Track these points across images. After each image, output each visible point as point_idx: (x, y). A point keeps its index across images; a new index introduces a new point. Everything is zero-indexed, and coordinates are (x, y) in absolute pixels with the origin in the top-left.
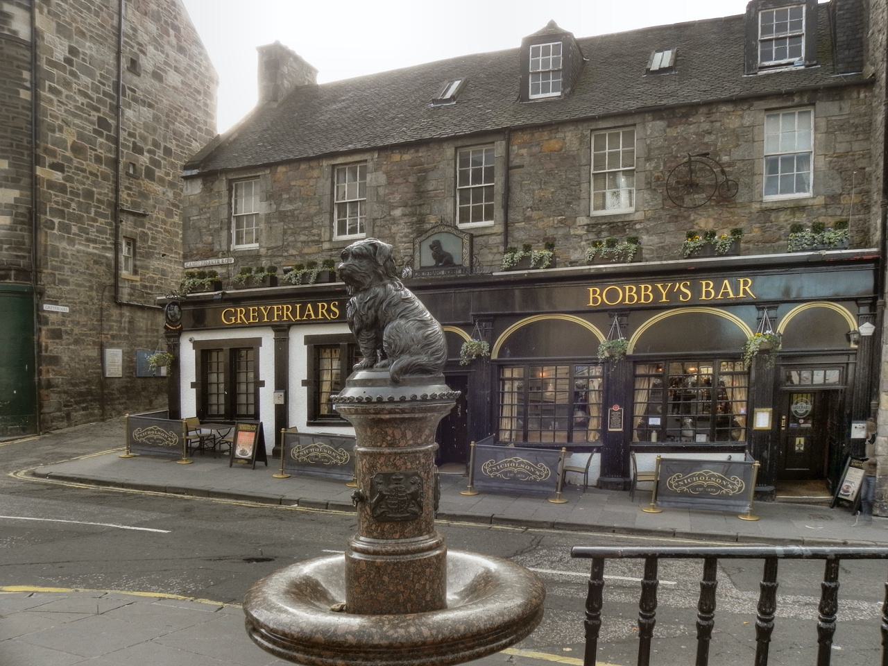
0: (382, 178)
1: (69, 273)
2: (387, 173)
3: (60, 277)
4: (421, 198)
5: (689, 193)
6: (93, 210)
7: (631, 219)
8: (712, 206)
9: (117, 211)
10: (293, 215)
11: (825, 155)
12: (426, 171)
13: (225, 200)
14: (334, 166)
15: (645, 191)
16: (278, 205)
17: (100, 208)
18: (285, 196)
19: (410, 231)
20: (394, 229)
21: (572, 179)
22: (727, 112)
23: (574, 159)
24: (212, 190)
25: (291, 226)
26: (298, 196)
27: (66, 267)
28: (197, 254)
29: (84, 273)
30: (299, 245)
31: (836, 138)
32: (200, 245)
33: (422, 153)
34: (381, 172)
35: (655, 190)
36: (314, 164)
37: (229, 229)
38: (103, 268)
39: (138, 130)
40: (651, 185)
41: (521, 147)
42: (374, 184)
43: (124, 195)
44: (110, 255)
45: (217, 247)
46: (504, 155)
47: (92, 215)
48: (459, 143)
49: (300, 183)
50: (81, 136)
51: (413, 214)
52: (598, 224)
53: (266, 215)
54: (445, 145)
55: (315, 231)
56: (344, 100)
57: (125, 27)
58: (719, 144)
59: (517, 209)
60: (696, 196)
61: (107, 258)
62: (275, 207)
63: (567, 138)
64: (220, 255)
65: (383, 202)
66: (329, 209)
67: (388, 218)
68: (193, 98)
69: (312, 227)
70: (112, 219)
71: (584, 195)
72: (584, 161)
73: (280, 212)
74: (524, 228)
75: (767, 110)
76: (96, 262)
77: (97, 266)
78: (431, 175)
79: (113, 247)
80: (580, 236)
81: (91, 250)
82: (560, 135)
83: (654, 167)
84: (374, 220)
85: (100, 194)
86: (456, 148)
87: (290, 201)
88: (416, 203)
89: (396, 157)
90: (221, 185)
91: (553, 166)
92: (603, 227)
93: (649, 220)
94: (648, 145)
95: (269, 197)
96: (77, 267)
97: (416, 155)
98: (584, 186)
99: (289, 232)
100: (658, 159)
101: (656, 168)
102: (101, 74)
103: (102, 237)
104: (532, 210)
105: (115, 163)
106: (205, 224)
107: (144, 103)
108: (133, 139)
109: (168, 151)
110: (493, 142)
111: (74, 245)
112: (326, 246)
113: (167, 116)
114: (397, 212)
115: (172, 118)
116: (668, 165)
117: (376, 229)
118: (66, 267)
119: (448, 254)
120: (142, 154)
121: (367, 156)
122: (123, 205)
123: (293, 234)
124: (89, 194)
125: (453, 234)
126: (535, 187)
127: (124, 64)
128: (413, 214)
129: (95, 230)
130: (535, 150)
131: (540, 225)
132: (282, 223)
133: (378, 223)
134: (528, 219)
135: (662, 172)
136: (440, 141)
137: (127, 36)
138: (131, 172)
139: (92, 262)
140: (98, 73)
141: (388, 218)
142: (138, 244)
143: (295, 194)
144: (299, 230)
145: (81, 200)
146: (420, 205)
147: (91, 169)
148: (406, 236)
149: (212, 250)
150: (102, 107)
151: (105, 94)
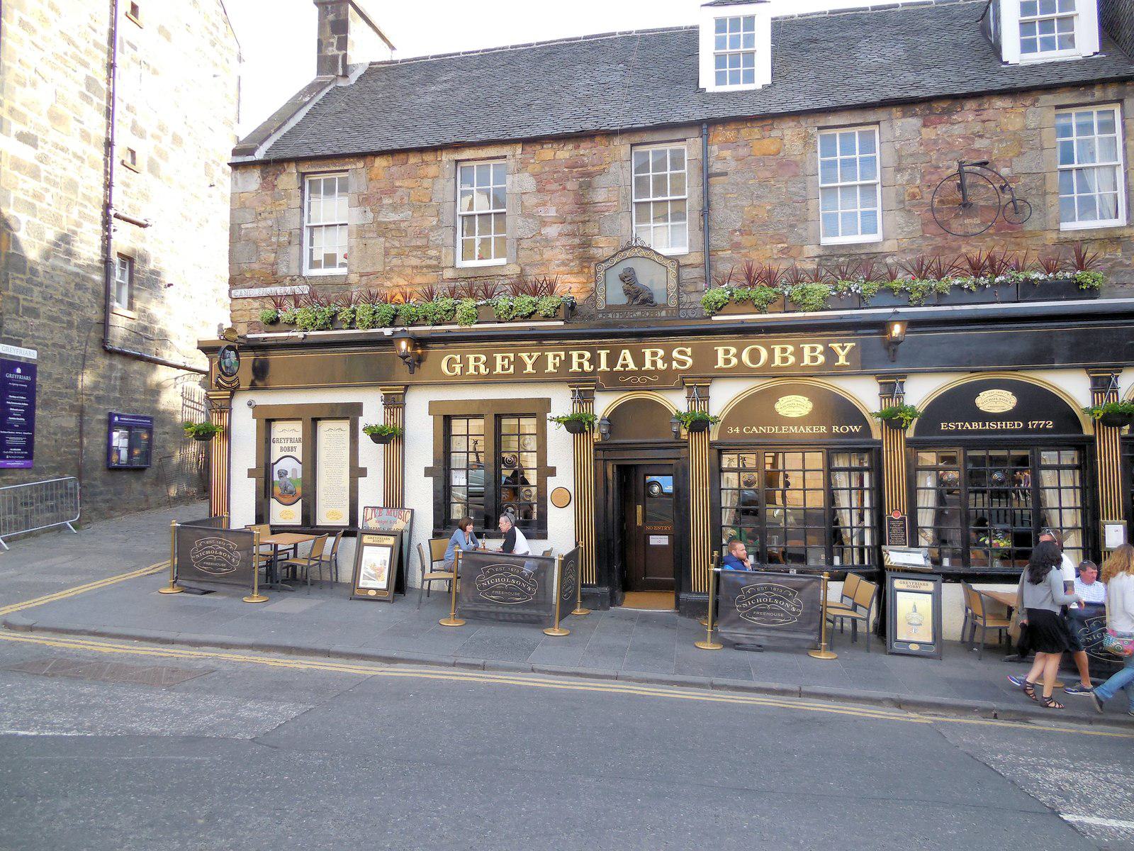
0: (529, 183)
1: (40, 299)
3: (25, 303)
4: (584, 212)
5: (957, 216)
7: (879, 250)
12: (590, 175)
13: (298, 202)
14: (457, 161)
16: (376, 212)
17: (86, 206)
19: (570, 257)
20: (548, 254)
21: (795, 194)
24: (275, 186)
25: (397, 244)
26: (406, 200)
27: (36, 290)
28: (252, 278)
29: (62, 301)
30: (409, 271)
32: (256, 266)
33: (586, 151)
34: (527, 174)
35: (909, 211)
36: (429, 157)
37: (301, 244)
38: (89, 296)
40: (907, 203)
42: (517, 190)
45: (282, 270)
46: (700, 157)
48: (636, 139)
49: (407, 183)
51: (572, 235)
52: (833, 256)
53: (358, 226)
54: (617, 141)
55: (432, 253)
56: (445, 81)
58: (995, 151)
59: (721, 232)
60: (967, 221)
61: (93, 281)
62: (371, 215)
64: (287, 281)
65: (531, 216)
66: (451, 220)
67: (538, 238)
69: (427, 247)
71: (811, 216)
72: (810, 170)
73: (380, 223)
74: (731, 258)
75: (1057, 107)
76: (79, 286)
77: (80, 293)
78: (599, 181)
79: (103, 266)
87: (394, 208)
88: (578, 219)
89: (547, 152)
91: (768, 174)
92: (842, 259)
94: (897, 151)
95: (364, 201)
96: (51, 291)
97: (576, 152)
99: (393, 252)
100: (912, 169)
101: (910, 182)
104: (742, 234)
106: (264, 235)
109: (177, 140)
112: (449, 274)
114: (552, 231)
116: (927, 178)
117: (522, 253)
118: (36, 290)
119: (646, 289)
121: (506, 150)
123: (399, 255)
126: (744, 203)
128: (573, 235)
130: (743, 152)
133: (525, 244)
134: (736, 246)
136: (610, 134)
139: (73, 285)
141: (538, 238)
142: (136, 266)
146: (584, 222)
148: (564, 264)
149: (274, 274)
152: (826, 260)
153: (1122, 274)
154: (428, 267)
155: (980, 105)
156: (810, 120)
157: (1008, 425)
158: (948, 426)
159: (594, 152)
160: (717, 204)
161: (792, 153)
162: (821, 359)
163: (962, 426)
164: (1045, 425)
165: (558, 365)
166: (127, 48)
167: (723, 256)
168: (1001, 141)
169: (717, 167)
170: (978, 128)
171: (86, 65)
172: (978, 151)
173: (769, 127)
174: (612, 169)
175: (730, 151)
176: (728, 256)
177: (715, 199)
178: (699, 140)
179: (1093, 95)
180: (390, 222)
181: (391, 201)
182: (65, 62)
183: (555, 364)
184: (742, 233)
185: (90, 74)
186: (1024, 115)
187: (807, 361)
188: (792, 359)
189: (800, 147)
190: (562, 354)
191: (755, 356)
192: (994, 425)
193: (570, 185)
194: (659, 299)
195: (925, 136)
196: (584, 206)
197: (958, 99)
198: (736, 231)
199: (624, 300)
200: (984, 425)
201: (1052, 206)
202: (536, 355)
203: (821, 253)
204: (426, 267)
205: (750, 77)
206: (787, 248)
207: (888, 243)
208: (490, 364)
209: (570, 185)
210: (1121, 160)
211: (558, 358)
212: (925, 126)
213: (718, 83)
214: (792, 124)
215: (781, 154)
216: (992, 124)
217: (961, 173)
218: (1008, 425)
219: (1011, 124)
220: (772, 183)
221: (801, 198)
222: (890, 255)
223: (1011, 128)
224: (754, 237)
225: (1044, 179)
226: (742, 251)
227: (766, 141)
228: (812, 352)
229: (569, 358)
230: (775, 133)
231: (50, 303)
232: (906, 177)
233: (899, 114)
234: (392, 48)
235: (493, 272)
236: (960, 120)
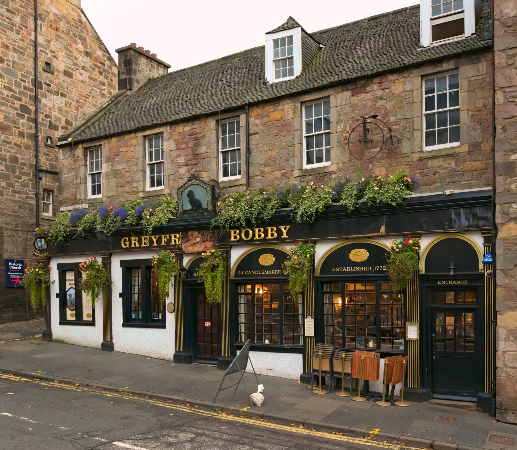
2: (175, 141)
5: (367, 148)
6: (17, 170)
8: (384, 158)
9: (38, 171)
10: (121, 173)
11: (468, 110)
13: (83, 163)
16: (113, 165)
18: (117, 159)
21: (289, 142)
22: (394, 80)
23: (290, 126)
25: (121, 181)
30: (125, 195)
31: (476, 95)
33: (197, 126)
35: (343, 147)
37: (85, 183)
39: (54, 113)
42: (168, 149)
43: (43, 159)
44: (33, 202)
45: (78, 197)
47: (17, 174)
50: (6, 118)
55: (135, 185)
57: (41, 40)
59: (255, 166)
60: (373, 150)
63: (285, 110)
68: (98, 88)
70: (33, 177)
71: (297, 153)
72: (297, 127)
74: (260, 179)
79: (35, 196)
81: (16, 198)
82: (281, 108)
84: (169, 175)
85: (23, 159)
86: (217, 121)
87: (119, 163)
90: (79, 151)
91: (277, 132)
92: (311, 177)
94: (338, 112)
98: (297, 147)
99: (119, 185)
100: (345, 122)
102: (21, 74)
103: (25, 190)
105: (35, 137)
107: (57, 93)
108: (49, 119)
110: (239, 116)
111: (2, 196)
112: (141, 195)
113: (78, 102)
115: (82, 103)
117: (170, 183)
120: (58, 130)
122: (42, 166)
123: (122, 186)
124: (14, 159)
125: (201, 186)
126: (266, 149)
127: (41, 64)
129: (19, 185)
130: (265, 120)
132: (115, 179)
134: (262, 173)
137: (42, 46)
138: (49, 143)
140: (19, 73)
142: (55, 194)
143: (122, 157)
144: (125, 183)
145: (8, 163)
147: (15, 142)
150: (23, 98)
151: (25, 88)
153: (454, 176)
154: (134, 192)
157: (364, 269)
158: (335, 269)
159: (200, 126)
161: (287, 118)
162: (276, 234)
163: (342, 269)
164: (383, 268)
165: (166, 241)
166: (44, 85)
169: (253, 129)
170: (379, 93)
171: (20, 100)
172: (379, 108)
174: (208, 135)
179: (442, 67)
180: (118, 170)
181: (118, 159)
182: (7, 100)
183: (165, 241)
184: (266, 165)
185: (23, 103)
187: (269, 236)
188: (263, 235)
189: (292, 115)
190: (168, 236)
191: (247, 234)
192: (359, 269)
193: (190, 145)
194: (204, 206)
195: (352, 102)
196: (196, 155)
197: (369, 78)
198: (262, 165)
200: (353, 269)
201: (417, 137)
202: (157, 236)
204: (132, 192)
205: (291, 73)
206: (285, 172)
207: (333, 166)
208: (140, 242)
209: (190, 145)
211: (166, 238)
212: (353, 96)
213: (276, 78)
215: (283, 120)
217: (364, 124)
218: (364, 269)
220: (279, 136)
223: (397, 92)
227: (276, 113)
228: (272, 232)
229: (170, 237)
231: (5, 216)
232: (342, 126)
234: (167, 67)
235: (159, 193)
236: (370, 90)
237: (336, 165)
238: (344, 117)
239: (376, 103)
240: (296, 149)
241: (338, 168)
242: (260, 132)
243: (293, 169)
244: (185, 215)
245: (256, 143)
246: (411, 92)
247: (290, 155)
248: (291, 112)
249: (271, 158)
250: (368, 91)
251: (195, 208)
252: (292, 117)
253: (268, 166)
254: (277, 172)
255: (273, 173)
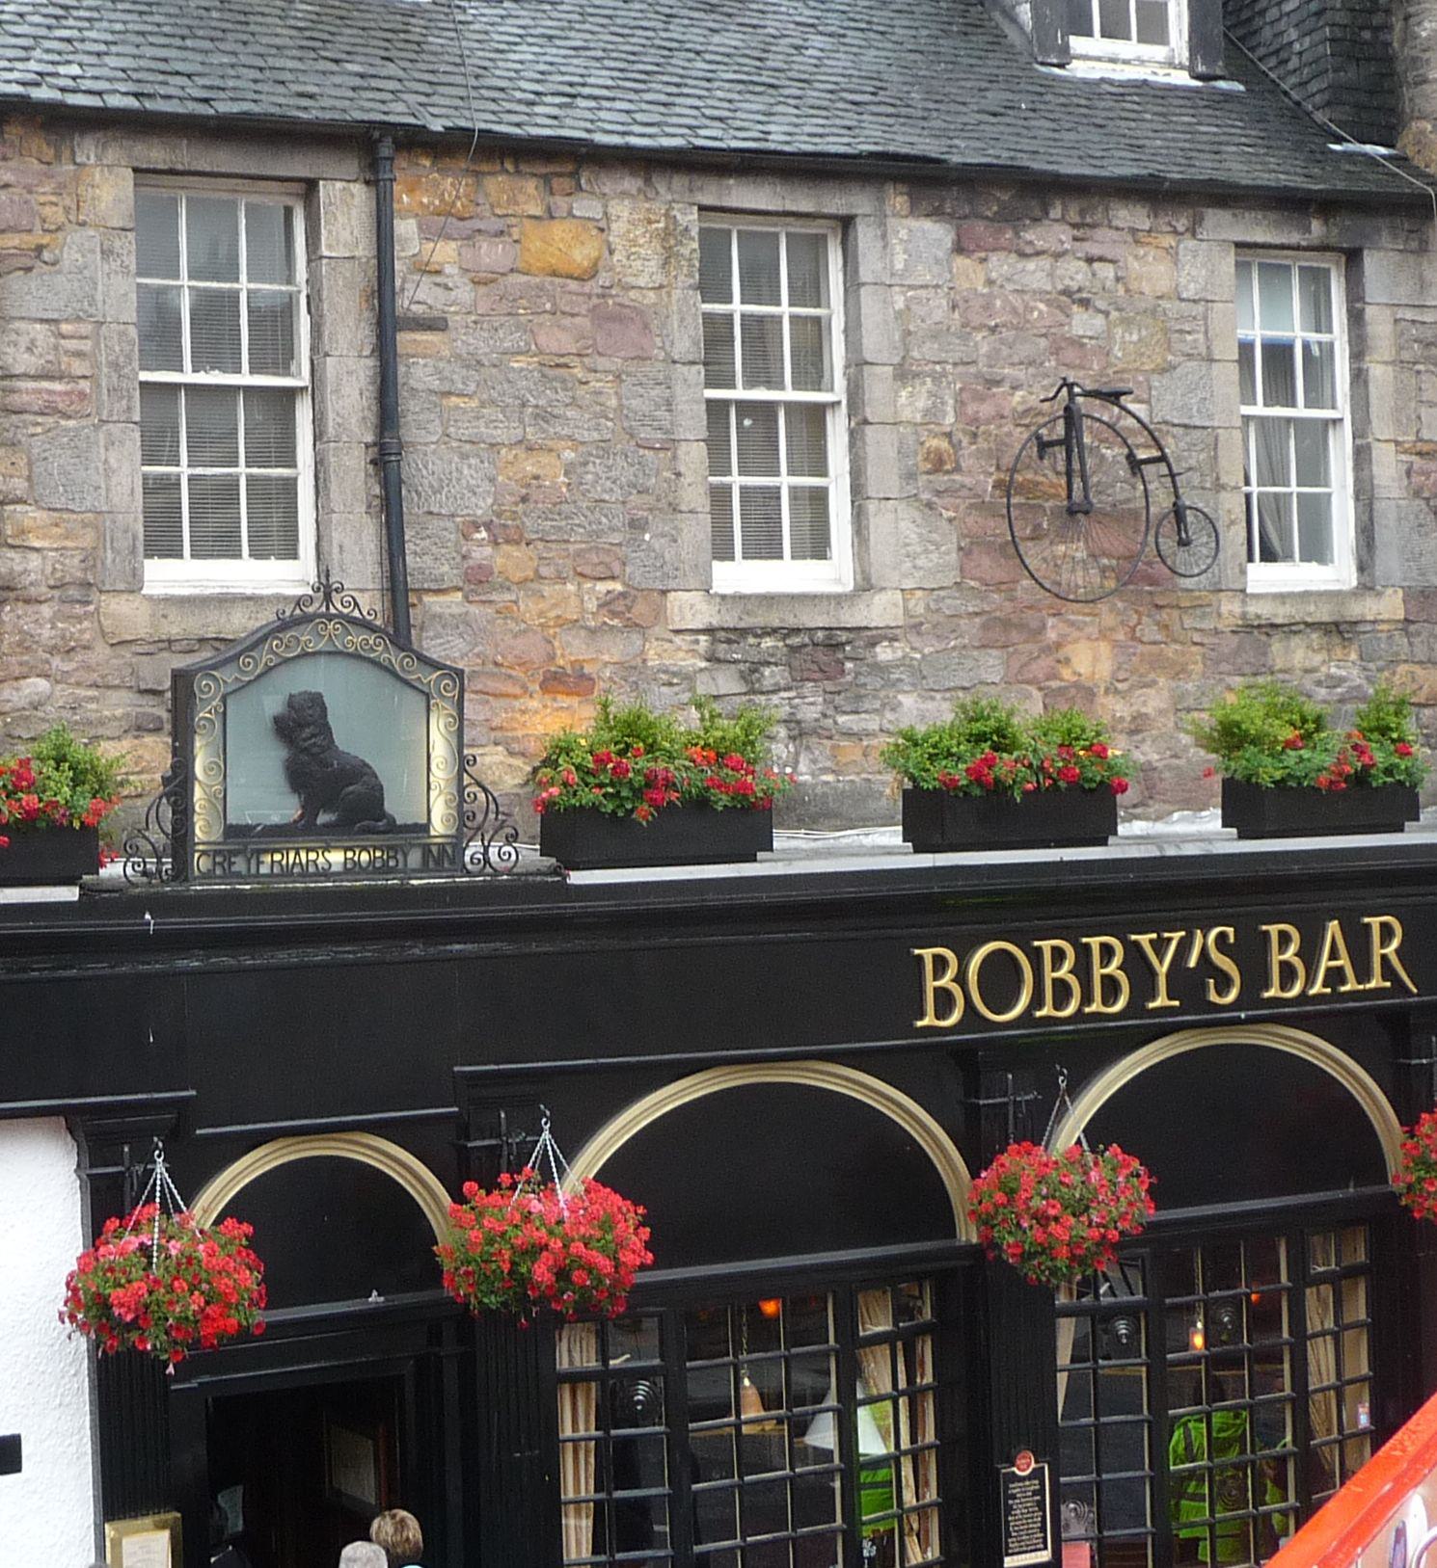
11: (1397, 443)
15: (901, 506)
35: (930, 505)
41: (440, 223)
46: (365, 250)
48: (156, 154)
52: (743, 632)
54: (86, 148)
59: (434, 525)
74: (465, 620)
80: (688, 678)
83: (926, 412)
92: (768, 643)
93: (916, 628)
100: (937, 378)
101: (932, 415)
116: (971, 409)
126: (500, 434)
130: (492, 254)
131: (528, 607)
134: (477, 580)
135: (949, 435)
152: (729, 641)
155: (1082, 213)
156: (679, 182)
160: (420, 427)
161: (631, 280)
167: (438, 609)
168: (1127, 322)
169: (415, 296)
170: (1074, 272)
173: (567, 183)
174: (70, 256)
175: (453, 245)
176: (456, 610)
177: (412, 409)
178: (358, 189)
186: (1172, 254)
189: (653, 265)
198: (477, 528)
199: (285, 809)
203: (715, 623)
206: (623, 595)
210: (1343, 409)
212: (959, 249)
214: (631, 183)
215: (604, 279)
216: (1107, 271)
219: (1149, 280)
220: (579, 373)
221: (659, 435)
222: (885, 638)
223: (1146, 289)
224: (530, 551)
225: (1216, 448)
226: (494, 597)
227: (559, 230)
230: (586, 207)
232: (922, 403)
233: (898, 201)
236: (1040, 244)
237: (899, 595)
238: (929, 350)
239: (1062, 318)
240: (682, 469)
241: (906, 610)
242: (454, 321)
243: (672, 584)
244: (239, 865)
245: (436, 384)
246: (1200, 308)
247: (649, 499)
248: (650, 252)
249: (535, 495)
250: (1029, 250)
251: (323, 818)
252: (659, 279)
253: (507, 542)
254: (571, 587)
255: (547, 590)
